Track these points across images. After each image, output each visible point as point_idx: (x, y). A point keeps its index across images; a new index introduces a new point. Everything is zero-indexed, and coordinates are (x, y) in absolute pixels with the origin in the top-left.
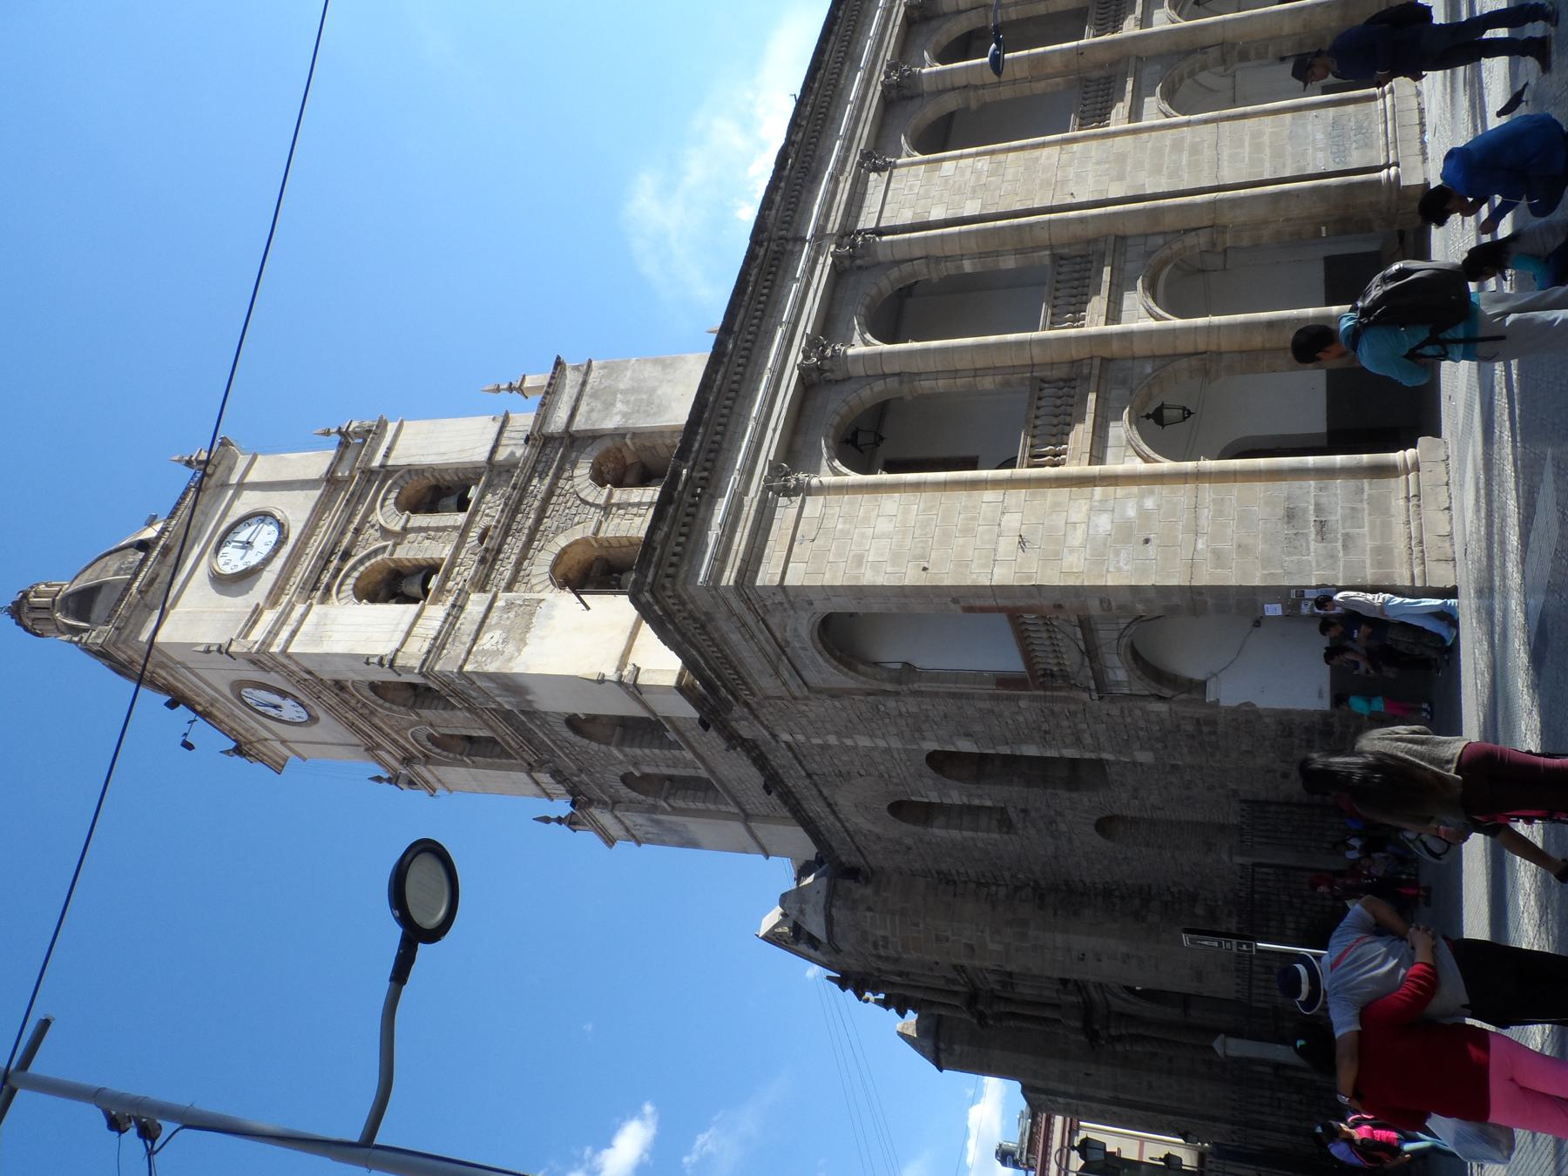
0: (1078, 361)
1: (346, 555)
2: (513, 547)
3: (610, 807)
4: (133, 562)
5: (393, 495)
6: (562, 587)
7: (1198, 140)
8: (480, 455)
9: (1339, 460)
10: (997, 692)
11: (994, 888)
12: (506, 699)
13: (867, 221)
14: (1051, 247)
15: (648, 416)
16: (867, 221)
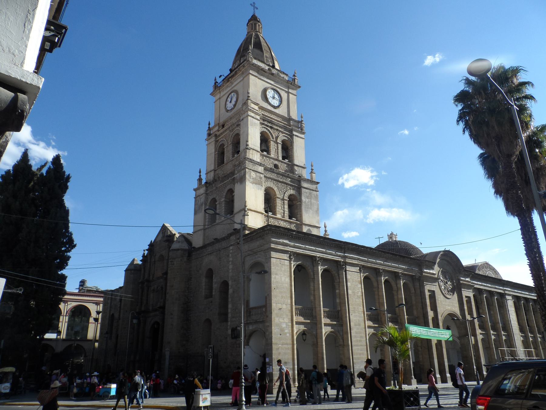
0: (316, 318)
1: (271, 128)
2: (274, 176)
3: (206, 193)
4: (269, 61)
5: (286, 138)
6: (265, 191)
7: (363, 341)
8: (296, 162)
9: (296, 372)
10: (245, 301)
11: (187, 291)
12: (238, 177)
13: (348, 268)
14: (341, 310)
15: (305, 208)
16: (348, 268)
